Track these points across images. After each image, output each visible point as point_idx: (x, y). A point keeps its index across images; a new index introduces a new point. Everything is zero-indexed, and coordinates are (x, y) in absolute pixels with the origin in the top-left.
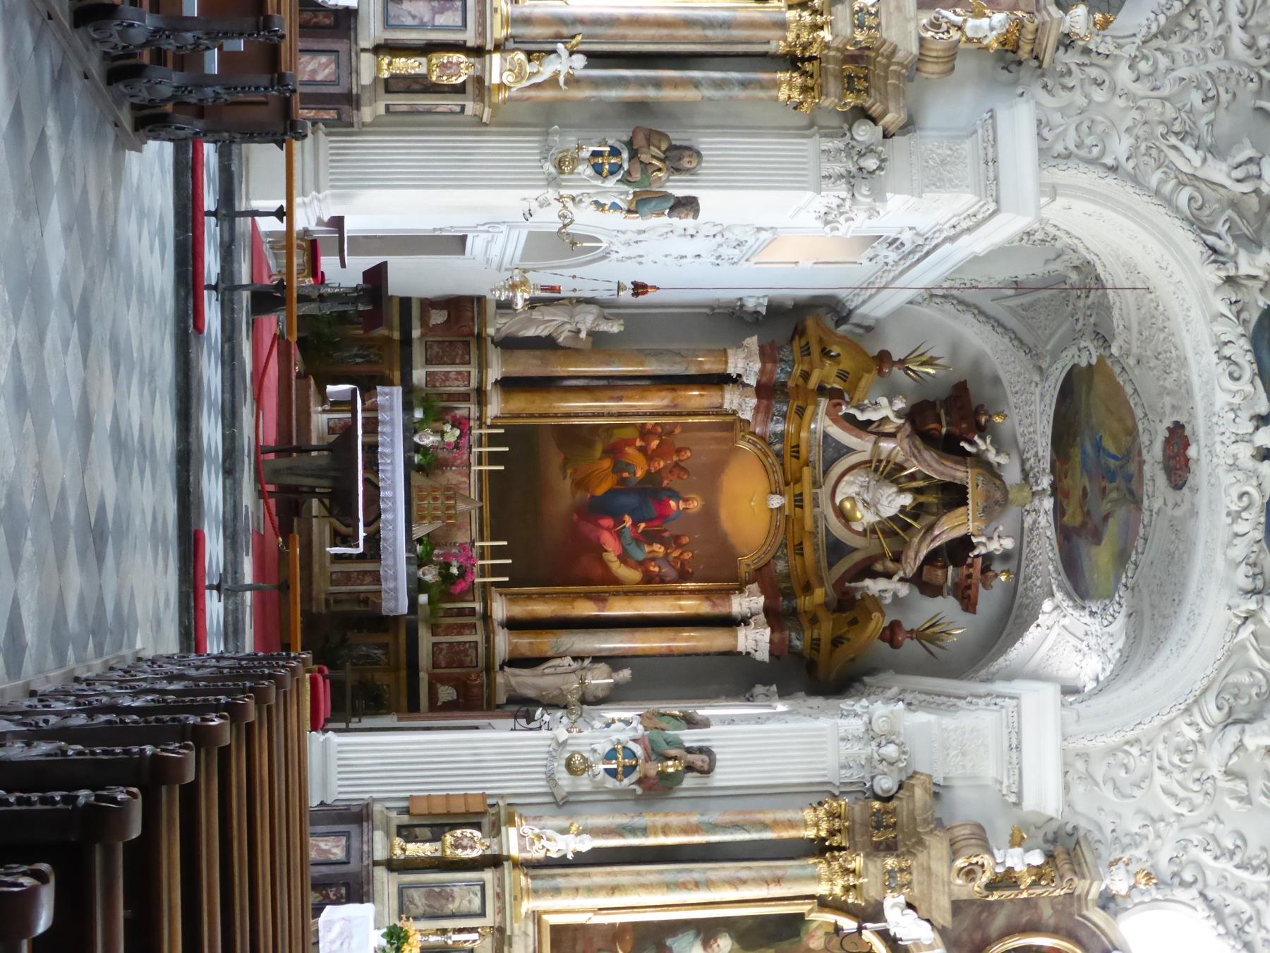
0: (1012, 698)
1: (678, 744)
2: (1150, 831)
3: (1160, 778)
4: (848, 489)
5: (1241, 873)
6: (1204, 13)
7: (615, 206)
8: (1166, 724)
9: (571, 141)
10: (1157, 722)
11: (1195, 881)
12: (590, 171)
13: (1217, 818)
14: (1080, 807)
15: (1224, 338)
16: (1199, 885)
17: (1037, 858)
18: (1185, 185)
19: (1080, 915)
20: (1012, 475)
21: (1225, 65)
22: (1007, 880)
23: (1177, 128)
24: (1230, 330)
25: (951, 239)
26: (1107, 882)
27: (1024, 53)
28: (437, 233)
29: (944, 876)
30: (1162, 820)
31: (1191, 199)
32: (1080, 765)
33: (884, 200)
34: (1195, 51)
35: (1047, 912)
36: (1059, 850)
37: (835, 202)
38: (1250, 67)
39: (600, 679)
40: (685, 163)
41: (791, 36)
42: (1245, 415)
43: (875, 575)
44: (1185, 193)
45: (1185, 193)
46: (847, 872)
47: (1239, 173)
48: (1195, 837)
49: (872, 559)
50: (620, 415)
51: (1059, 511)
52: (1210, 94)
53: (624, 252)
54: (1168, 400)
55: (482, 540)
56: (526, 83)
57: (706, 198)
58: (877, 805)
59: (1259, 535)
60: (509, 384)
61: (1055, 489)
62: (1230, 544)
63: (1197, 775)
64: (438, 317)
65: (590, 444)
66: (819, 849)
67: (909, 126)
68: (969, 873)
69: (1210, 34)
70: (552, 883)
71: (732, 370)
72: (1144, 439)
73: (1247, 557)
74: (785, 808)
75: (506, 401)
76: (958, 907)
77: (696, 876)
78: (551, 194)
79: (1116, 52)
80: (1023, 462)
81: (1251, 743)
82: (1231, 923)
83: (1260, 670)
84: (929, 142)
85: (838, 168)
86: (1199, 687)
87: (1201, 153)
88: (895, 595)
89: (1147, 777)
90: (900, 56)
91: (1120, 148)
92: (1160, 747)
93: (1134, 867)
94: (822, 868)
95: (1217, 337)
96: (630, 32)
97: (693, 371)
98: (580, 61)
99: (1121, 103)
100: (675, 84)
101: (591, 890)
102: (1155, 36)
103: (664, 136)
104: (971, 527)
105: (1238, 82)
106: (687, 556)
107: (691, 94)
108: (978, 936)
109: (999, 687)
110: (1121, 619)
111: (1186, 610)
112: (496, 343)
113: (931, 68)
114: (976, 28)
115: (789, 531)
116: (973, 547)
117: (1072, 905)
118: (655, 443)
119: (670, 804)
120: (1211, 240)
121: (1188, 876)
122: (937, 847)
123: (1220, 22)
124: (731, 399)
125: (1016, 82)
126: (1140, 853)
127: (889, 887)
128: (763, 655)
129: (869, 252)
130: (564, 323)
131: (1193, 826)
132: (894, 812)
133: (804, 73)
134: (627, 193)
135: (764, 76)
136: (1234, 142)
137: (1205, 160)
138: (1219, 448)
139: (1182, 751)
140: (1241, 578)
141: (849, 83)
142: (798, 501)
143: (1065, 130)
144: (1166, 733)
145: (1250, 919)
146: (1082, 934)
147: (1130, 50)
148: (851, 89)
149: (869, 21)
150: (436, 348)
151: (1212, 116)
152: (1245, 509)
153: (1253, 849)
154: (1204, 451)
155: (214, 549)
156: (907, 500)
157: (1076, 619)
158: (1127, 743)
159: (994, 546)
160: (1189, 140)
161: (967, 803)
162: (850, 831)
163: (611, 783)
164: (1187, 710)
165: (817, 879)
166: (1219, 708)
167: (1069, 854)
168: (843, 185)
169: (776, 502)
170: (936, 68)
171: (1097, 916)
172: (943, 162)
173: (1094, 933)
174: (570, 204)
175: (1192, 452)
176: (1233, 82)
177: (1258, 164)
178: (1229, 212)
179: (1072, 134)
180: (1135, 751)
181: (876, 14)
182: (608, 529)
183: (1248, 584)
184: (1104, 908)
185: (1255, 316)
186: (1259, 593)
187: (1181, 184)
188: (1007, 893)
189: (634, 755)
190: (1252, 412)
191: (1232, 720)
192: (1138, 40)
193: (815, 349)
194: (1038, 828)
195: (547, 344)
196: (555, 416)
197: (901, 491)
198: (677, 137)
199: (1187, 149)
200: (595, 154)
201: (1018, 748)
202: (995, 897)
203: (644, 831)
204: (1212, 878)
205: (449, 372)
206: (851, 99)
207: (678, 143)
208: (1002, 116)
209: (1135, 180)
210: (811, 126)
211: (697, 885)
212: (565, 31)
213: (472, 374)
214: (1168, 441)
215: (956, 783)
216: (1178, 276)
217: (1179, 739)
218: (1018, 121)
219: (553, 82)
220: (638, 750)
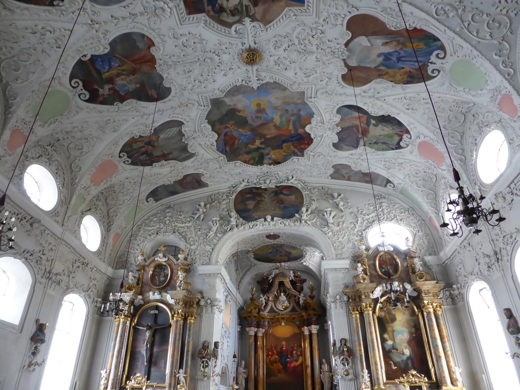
1: (340, 347)
2: (352, 241)
4: (280, 307)
5: (359, 223)
6: (182, 231)
7: (215, 362)
8: (329, 238)
9: (200, 373)
12: (207, 369)
13: (348, 228)
14: (347, 256)
17: (359, 265)
20: (277, 271)
21: (193, 227)
22: (365, 271)
24: (247, 226)
25: (226, 284)
27: (187, 268)
29: (365, 284)
32: (339, 256)
33: (217, 298)
35: (371, 262)
36: (357, 260)
37: (217, 310)
39: (326, 367)
40: (206, 345)
41: (180, 319)
42: (264, 223)
43: (299, 301)
44: (218, 235)
45: (218, 235)
46: (366, 307)
47: (215, 224)
48: (352, 232)
49: (295, 301)
50: (263, 362)
51: (284, 261)
53: (226, 360)
54: (261, 239)
56: (185, 385)
57: (215, 340)
58: (350, 300)
59: (289, 220)
61: (280, 262)
62: (291, 226)
66: (361, 314)
67: (201, 293)
68: (364, 279)
70: (376, 380)
71: (253, 334)
72: (269, 243)
74: (353, 321)
76: (371, 282)
77: (371, 343)
78: (212, 379)
80: (274, 269)
81: (332, 221)
82: (369, 225)
84: (205, 288)
85: (210, 309)
86: (321, 232)
88: (303, 297)
89: (340, 242)
90: (186, 294)
91: (208, 248)
94: (366, 313)
96: (175, 358)
97: (253, 343)
98: (181, 371)
99: (199, 248)
100: (188, 347)
101: (377, 370)
103: (200, 350)
104: (288, 280)
106: (296, 345)
108: (378, 277)
109: (323, 273)
110: (307, 248)
111: (304, 234)
114: (181, 278)
115: (290, 321)
116: (292, 280)
118: (270, 353)
119: (354, 349)
120: (228, 230)
121: (360, 233)
122: (359, 286)
124: (260, 334)
125: (193, 270)
126: (356, 243)
128: (318, 327)
129: (228, 302)
132: (352, 296)
133: (188, 316)
139: (334, 235)
140: (298, 224)
141: (191, 306)
142: (283, 318)
146: (375, 255)
147: (188, 246)
148: (192, 306)
149: (178, 301)
153: (353, 221)
156: (282, 294)
157: (307, 257)
158: (333, 245)
159: (292, 275)
161: (348, 280)
162: (357, 306)
163: (350, 364)
164: (326, 234)
165: (369, 314)
168: (213, 308)
169: (283, 324)
171: (370, 252)
172: (210, 285)
174: (214, 374)
175: (272, 234)
179: (205, 258)
180: (335, 245)
183: (299, 222)
184: (369, 250)
187: (217, 236)
189: (343, 359)
191: (327, 225)
193: (249, 314)
195: (247, 380)
196: (264, 378)
197: (280, 295)
198: (200, 347)
199: (210, 234)
200: (203, 367)
201: (336, 269)
203: (361, 356)
204: (361, 229)
206: (195, 306)
208: (200, 273)
209: (215, 245)
210: (200, 315)
211: (373, 343)
212: (174, 374)
214: (270, 239)
215: (344, 282)
216: (235, 236)
218: (202, 269)
220: (342, 357)
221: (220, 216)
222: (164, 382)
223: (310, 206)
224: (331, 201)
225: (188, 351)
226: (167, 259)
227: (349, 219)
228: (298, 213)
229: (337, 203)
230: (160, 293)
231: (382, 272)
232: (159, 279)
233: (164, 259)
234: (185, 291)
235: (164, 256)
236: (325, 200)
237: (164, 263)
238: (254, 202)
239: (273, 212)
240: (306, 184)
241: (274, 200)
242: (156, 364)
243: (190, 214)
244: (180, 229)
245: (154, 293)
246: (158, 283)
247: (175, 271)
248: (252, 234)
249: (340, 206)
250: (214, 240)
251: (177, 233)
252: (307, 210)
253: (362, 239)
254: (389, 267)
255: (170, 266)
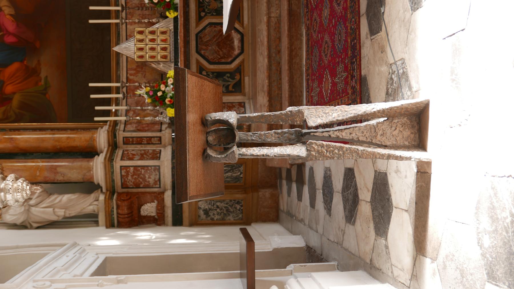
28: (122, 277)
55: (117, 24)
60: (90, 153)
64: (149, 209)
65: (23, 106)
75: (93, 140)
112: (98, 187)
130: (36, 205)
150: (151, 181)
182: (9, 33)
205: (140, 159)
213: (119, 158)
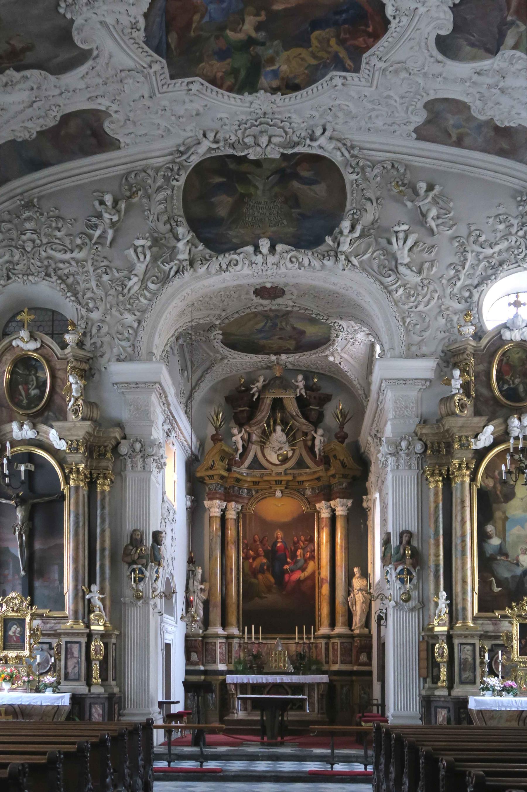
0: (382, 383)
3: (421, 308)
5: (467, 267)
6: (66, 271)
10: (395, 309)
11: (469, 290)
15: (218, 268)
16: (471, 288)
18: (147, 285)
19: (483, 350)
21: (90, 262)
23: (120, 289)
24: (214, 264)
26: (468, 336)
27: (86, 367)
30: (440, 307)
31: (153, 283)
33: (155, 440)
34: (84, 277)
35: (481, 367)
38: (91, 248)
46: (460, 468)
52: (104, 270)
62: (314, 268)
63: (420, 288)
68: (463, 407)
69: (75, 269)
73: (320, 259)
76: (477, 413)
79: (85, 319)
81: (407, 260)
83: (372, 254)
86: (379, 287)
87: (132, 277)
91: (129, 318)
92: (406, 307)
93: (463, 323)
94: (458, 480)
95: (217, 271)
96: (81, 562)
102: (77, 298)
105: (98, 256)
107: (107, 533)
111: (343, 291)
113: (96, 415)
117: (478, 354)
120: (172, 273)
121: (467, 294)
122: (450, 423)
123: (70, 263)
125: (99, 371)
126: (455, 318)
127: (468, 447)
131: (444, 290)
133: (98, 478)
134: (151, 566)
135: (99, 497)
136: (126, 258)
137: (136, 275)
138: (269, 273)
139: (409, 296)
141: (102, 456)
143: (122, 347)
144: (400, 304)
145: (488, 262)
148: (105, 455)
151: (114, 270)
152: (298, 260)
154: (270, 280)
155: (312, 766)
158: (404, 323)
160: (126, 282)
161: (431, 406)
164: (390, 292)
165: (463, 483)
166: (389, 276)
167: (455, 355)
170: (95, 412)
173: (492, 344)
176: (98, 258)
177: (137, 247)
178: (159, 263)
179: (123, 343)
180: (408, 320)
181: (72, 441)
184: (480, 338)
185: (208, 251)
186: (337, 253)
187: (146, 288)
188: (472, 387)
190: (253, 255)
191: (395, 270)
192: (79, 307)
194: (442, 371)
199: (131, 283)
202: (473, 393)
206: (109, 455)
207: (129, 541)
208: (116, 379)
210: (121, 475)
212: (80, 594)
216: (188, 290)
217: (403, 297)
219: (102, 600)
221: (151, 235)
222: (63, 608)
223: (361, 215)
224: (409, 204)
225: (103, 550)
226: (39, 345)
227: (448, 255)
228: (330, 234)
229: (424, 210)
230: (34, 426)
231: (501, 391)
232: (28, 394)
233: (33, 345)
234: (88, 423)
235: (33, 337)
236: (397, 201)
237: (35, 355)
238: (230, 200)
239: (274, 229)
240: (355, 152)
241: (276, 196)
242: (42, 574)
243: (80, 226)
244: (61, 265)
245: (22, 425)
246: (25, 401)
247: (60, 374)
248: (224, 285)
249: (429, 219)
250: (142, 299)
251: (55, 278)
252: (353, 228)
253: (471, 309)
254: (517, 381)
255: (48, 362)
